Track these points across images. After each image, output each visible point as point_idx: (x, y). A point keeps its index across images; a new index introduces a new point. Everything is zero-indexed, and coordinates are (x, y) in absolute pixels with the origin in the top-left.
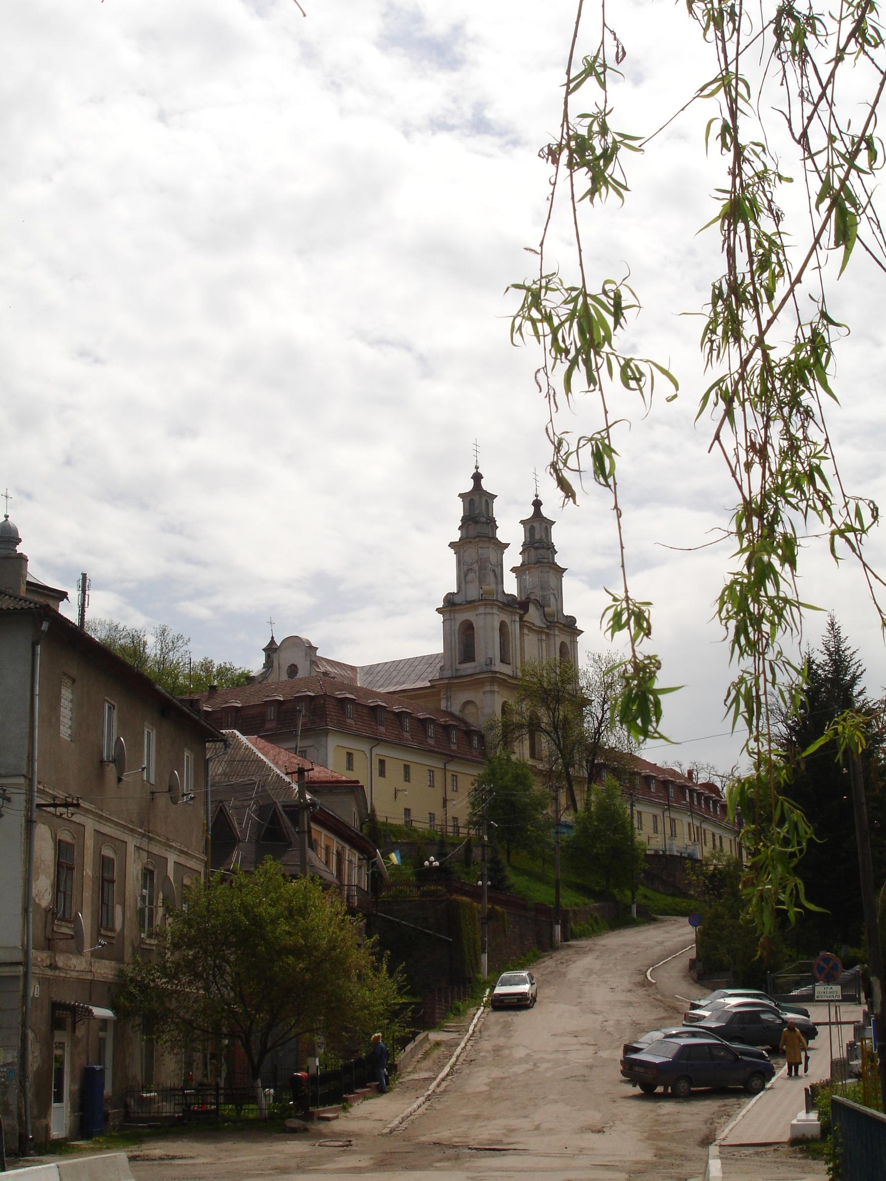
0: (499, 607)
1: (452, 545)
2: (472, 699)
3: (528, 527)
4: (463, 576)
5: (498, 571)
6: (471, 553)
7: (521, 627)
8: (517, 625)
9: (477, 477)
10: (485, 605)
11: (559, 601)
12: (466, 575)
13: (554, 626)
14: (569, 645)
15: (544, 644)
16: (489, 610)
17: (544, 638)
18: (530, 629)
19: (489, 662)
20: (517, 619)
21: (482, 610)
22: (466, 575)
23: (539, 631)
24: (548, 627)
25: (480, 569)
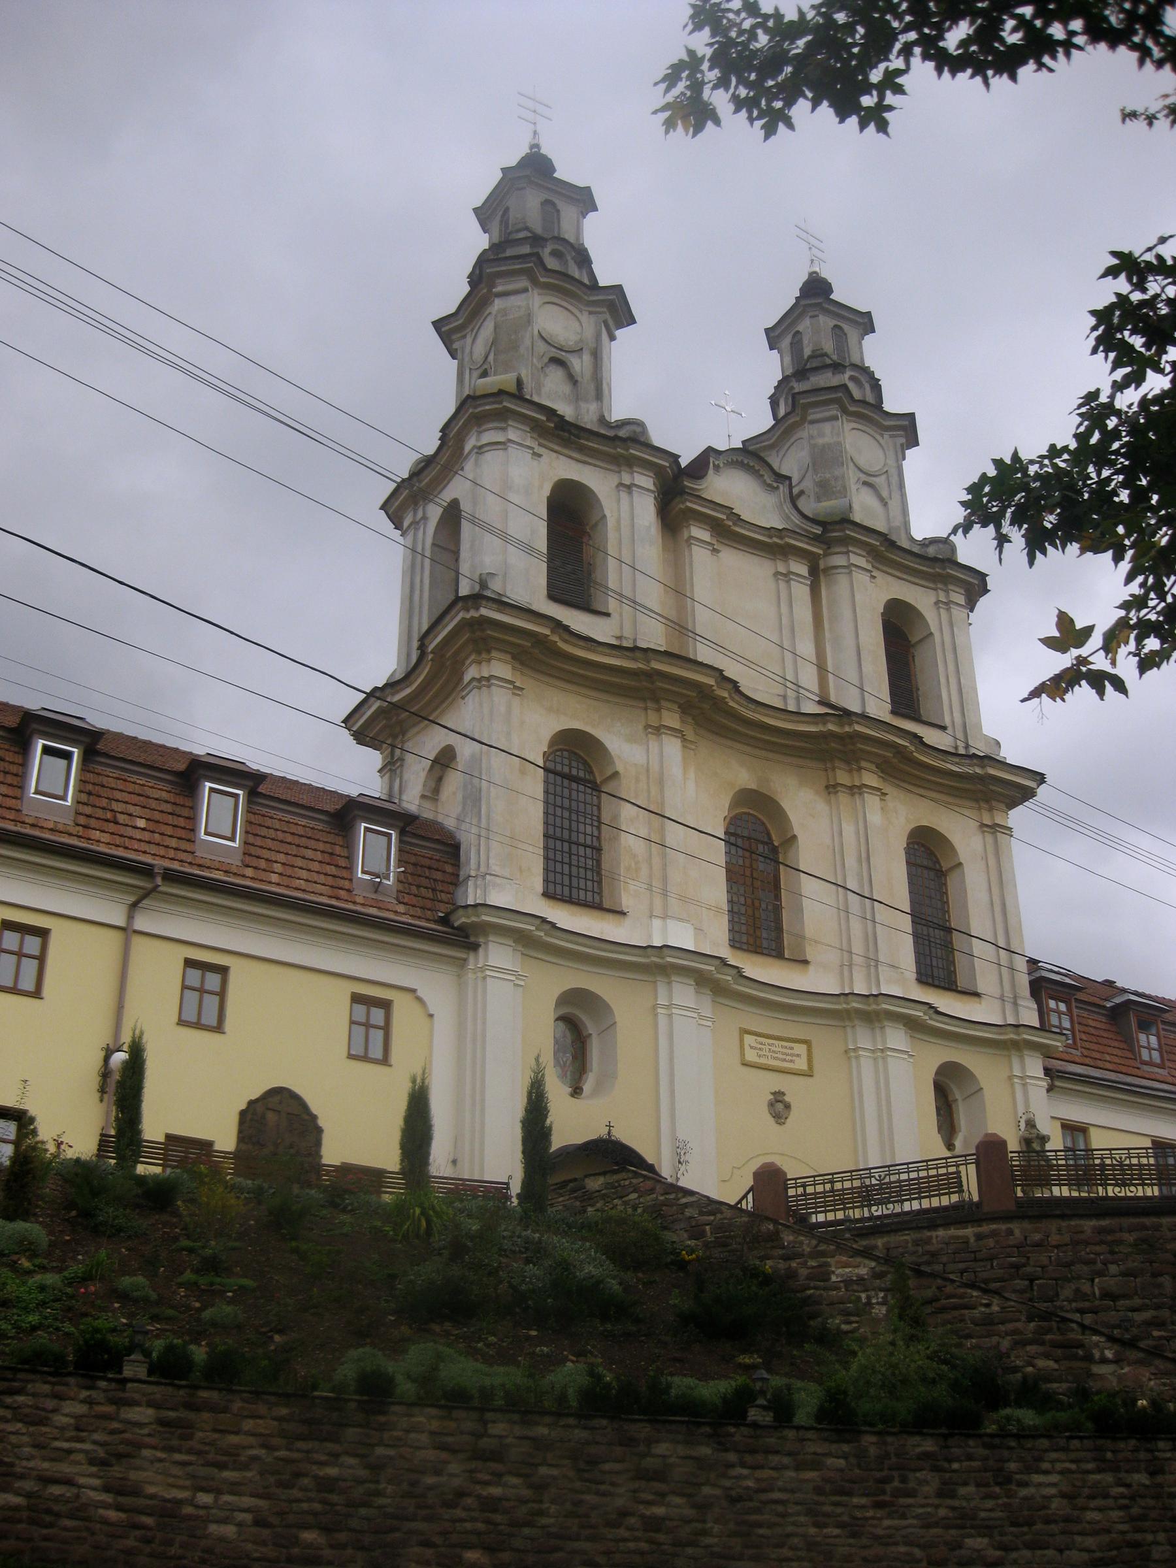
11: (894, 504)
13: (846, 541)
14: (929, 614)
15: (801, 591)
17: (802, 569)
23: (771, 546)
24: (816, 539)
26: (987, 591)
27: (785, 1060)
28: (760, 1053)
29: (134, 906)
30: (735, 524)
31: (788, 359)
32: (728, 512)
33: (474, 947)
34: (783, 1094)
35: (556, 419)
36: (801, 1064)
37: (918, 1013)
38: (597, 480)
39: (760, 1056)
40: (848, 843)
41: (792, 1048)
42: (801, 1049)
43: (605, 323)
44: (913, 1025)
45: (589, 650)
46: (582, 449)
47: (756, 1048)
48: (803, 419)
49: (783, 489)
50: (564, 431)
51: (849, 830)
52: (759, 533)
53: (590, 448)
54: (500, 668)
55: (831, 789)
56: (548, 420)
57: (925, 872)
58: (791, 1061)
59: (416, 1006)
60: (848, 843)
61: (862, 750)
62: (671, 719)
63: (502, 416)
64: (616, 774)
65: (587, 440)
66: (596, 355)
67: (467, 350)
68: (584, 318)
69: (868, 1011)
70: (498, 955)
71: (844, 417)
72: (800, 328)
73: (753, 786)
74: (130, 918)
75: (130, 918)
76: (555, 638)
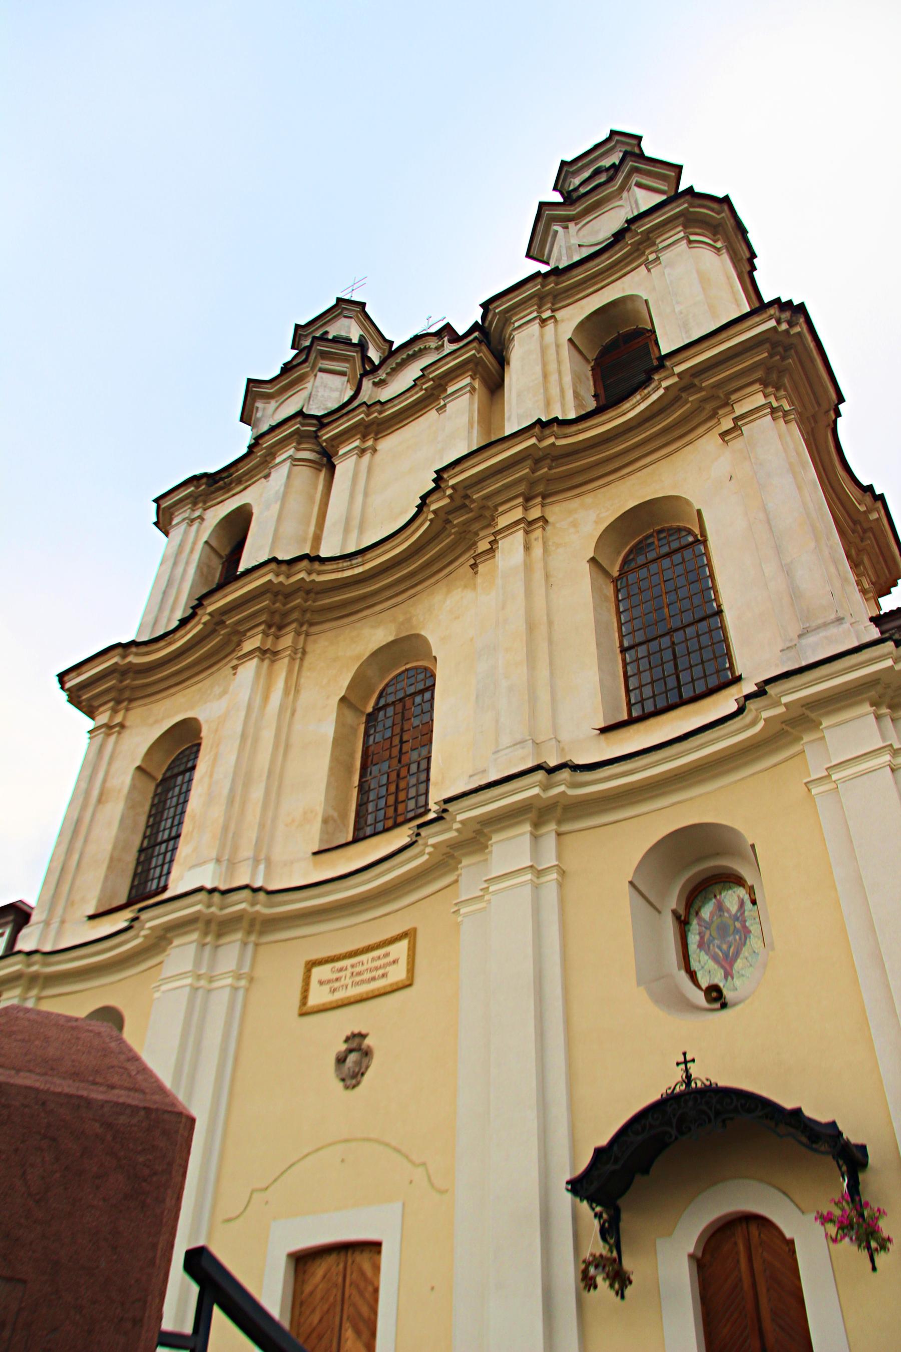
26: (726, 200)
27: (374, 979)
28: (336, 985)
30: (380, 413)
32: (364, 408)
34: (363, 1036)
35: (204, 480)
36: (398, 974)
37: (529, 790)
39: (335, 990)
41: (387, 955)
43: (321, 370)
44: (538, 814)
45: (170, 644)
46: (239, 481)
47: (329, 981)
50: (216, 482)
52: (412, 396)
53: (245, 474)
56: (197, 487)
57: (666, 563)
58: (383, 975)
61: (488, 497)
65: (237, 471)
71: (571, 225)
73: (391, 638)
76: (131, 659)
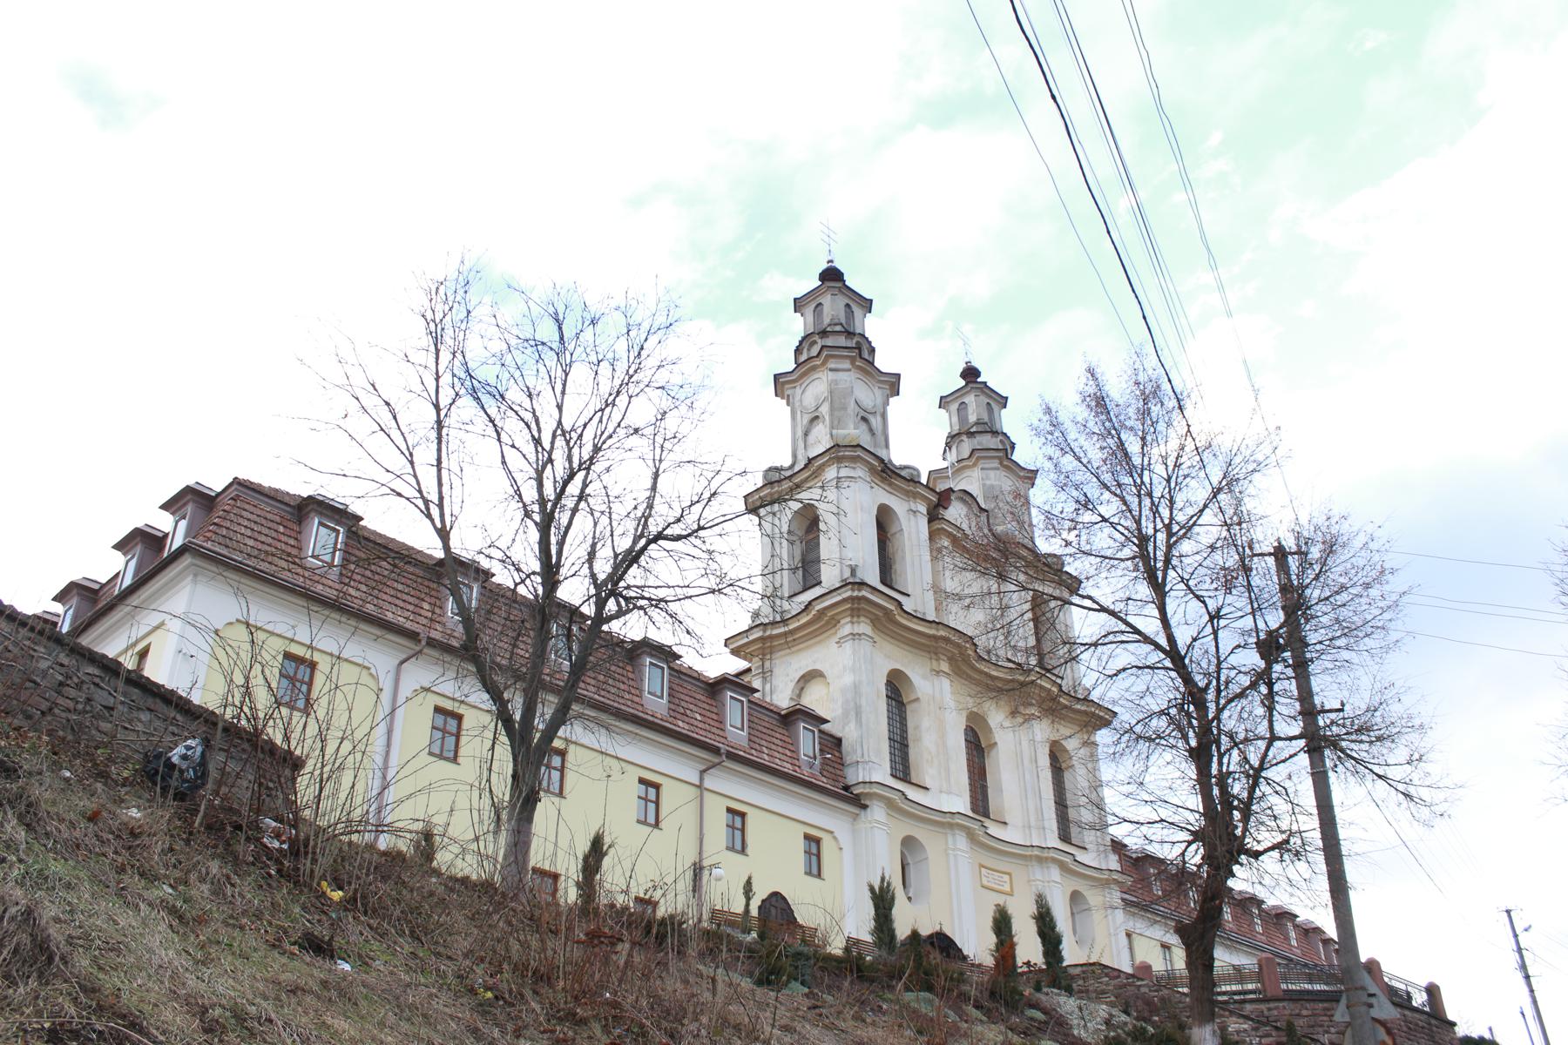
0: (872, 470)
1: (781, 383)
2: (818, 667)
3: (954, 407)
4: (800, 433)
5: (875, 422)
6: (816, 389)
7: (932, 536)
8: (923, 522)
9: (832, 276)
10: (839, 460)
12: (806, 434)
16: (844, 472)
18: (955, 540)
19: (847, 574)
20: (923, 509)
21: (831, 473)
22: (806, 434)
25: (832, 409)
29: (703, 772)
31: (955, 419)
33: (865, 807)
38: (898, 505)
40: (1020, 748)
42: (1006, 878)
46: (890, 484)
48: (975, 465)
49: (984, 517)
51: (1025, 744)
54: (864, 627)
55: (1014, 713)
59: (833, 843)
60: (1020, 748)
62: (945, 666)
63: (855, 459)
64: (917, 700)
66: (884, 416)
67: (798, 398)
68: (876, 390)
69: (1037, 856)
70: (877, 812)
72: (966, 400)
74: (701, 779)
75: (701, 779)
